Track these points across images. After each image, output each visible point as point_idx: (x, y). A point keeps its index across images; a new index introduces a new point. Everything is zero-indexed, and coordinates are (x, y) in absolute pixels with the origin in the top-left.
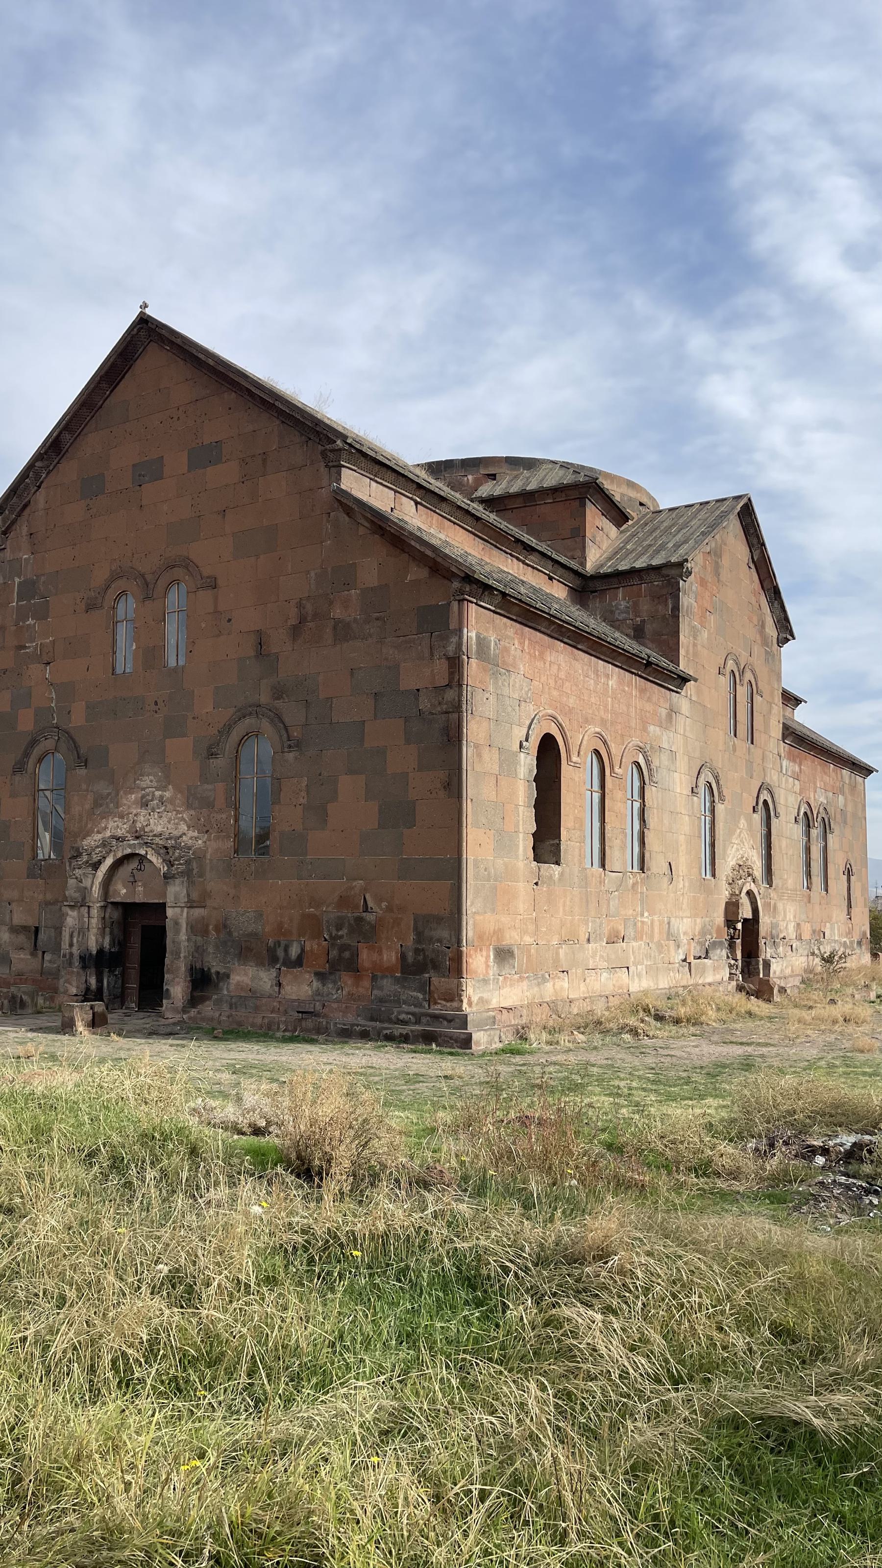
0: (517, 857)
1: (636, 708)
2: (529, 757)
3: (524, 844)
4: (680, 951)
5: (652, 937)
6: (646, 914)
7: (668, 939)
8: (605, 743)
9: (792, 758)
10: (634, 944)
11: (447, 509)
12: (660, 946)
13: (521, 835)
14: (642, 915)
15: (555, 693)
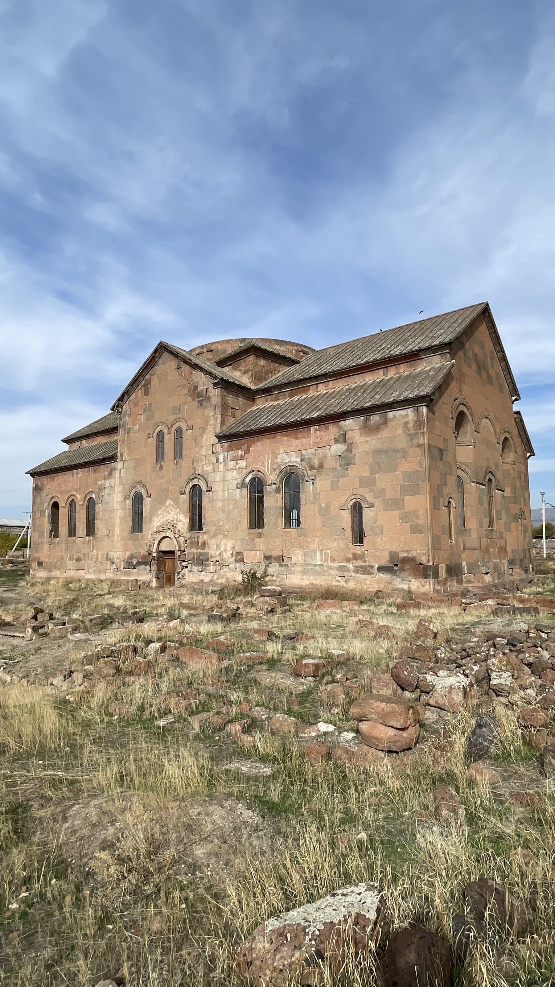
3: (47, 534)
6: (94, 551)
7: (107, 560)
12: (101, 563)
14: (92, 551)
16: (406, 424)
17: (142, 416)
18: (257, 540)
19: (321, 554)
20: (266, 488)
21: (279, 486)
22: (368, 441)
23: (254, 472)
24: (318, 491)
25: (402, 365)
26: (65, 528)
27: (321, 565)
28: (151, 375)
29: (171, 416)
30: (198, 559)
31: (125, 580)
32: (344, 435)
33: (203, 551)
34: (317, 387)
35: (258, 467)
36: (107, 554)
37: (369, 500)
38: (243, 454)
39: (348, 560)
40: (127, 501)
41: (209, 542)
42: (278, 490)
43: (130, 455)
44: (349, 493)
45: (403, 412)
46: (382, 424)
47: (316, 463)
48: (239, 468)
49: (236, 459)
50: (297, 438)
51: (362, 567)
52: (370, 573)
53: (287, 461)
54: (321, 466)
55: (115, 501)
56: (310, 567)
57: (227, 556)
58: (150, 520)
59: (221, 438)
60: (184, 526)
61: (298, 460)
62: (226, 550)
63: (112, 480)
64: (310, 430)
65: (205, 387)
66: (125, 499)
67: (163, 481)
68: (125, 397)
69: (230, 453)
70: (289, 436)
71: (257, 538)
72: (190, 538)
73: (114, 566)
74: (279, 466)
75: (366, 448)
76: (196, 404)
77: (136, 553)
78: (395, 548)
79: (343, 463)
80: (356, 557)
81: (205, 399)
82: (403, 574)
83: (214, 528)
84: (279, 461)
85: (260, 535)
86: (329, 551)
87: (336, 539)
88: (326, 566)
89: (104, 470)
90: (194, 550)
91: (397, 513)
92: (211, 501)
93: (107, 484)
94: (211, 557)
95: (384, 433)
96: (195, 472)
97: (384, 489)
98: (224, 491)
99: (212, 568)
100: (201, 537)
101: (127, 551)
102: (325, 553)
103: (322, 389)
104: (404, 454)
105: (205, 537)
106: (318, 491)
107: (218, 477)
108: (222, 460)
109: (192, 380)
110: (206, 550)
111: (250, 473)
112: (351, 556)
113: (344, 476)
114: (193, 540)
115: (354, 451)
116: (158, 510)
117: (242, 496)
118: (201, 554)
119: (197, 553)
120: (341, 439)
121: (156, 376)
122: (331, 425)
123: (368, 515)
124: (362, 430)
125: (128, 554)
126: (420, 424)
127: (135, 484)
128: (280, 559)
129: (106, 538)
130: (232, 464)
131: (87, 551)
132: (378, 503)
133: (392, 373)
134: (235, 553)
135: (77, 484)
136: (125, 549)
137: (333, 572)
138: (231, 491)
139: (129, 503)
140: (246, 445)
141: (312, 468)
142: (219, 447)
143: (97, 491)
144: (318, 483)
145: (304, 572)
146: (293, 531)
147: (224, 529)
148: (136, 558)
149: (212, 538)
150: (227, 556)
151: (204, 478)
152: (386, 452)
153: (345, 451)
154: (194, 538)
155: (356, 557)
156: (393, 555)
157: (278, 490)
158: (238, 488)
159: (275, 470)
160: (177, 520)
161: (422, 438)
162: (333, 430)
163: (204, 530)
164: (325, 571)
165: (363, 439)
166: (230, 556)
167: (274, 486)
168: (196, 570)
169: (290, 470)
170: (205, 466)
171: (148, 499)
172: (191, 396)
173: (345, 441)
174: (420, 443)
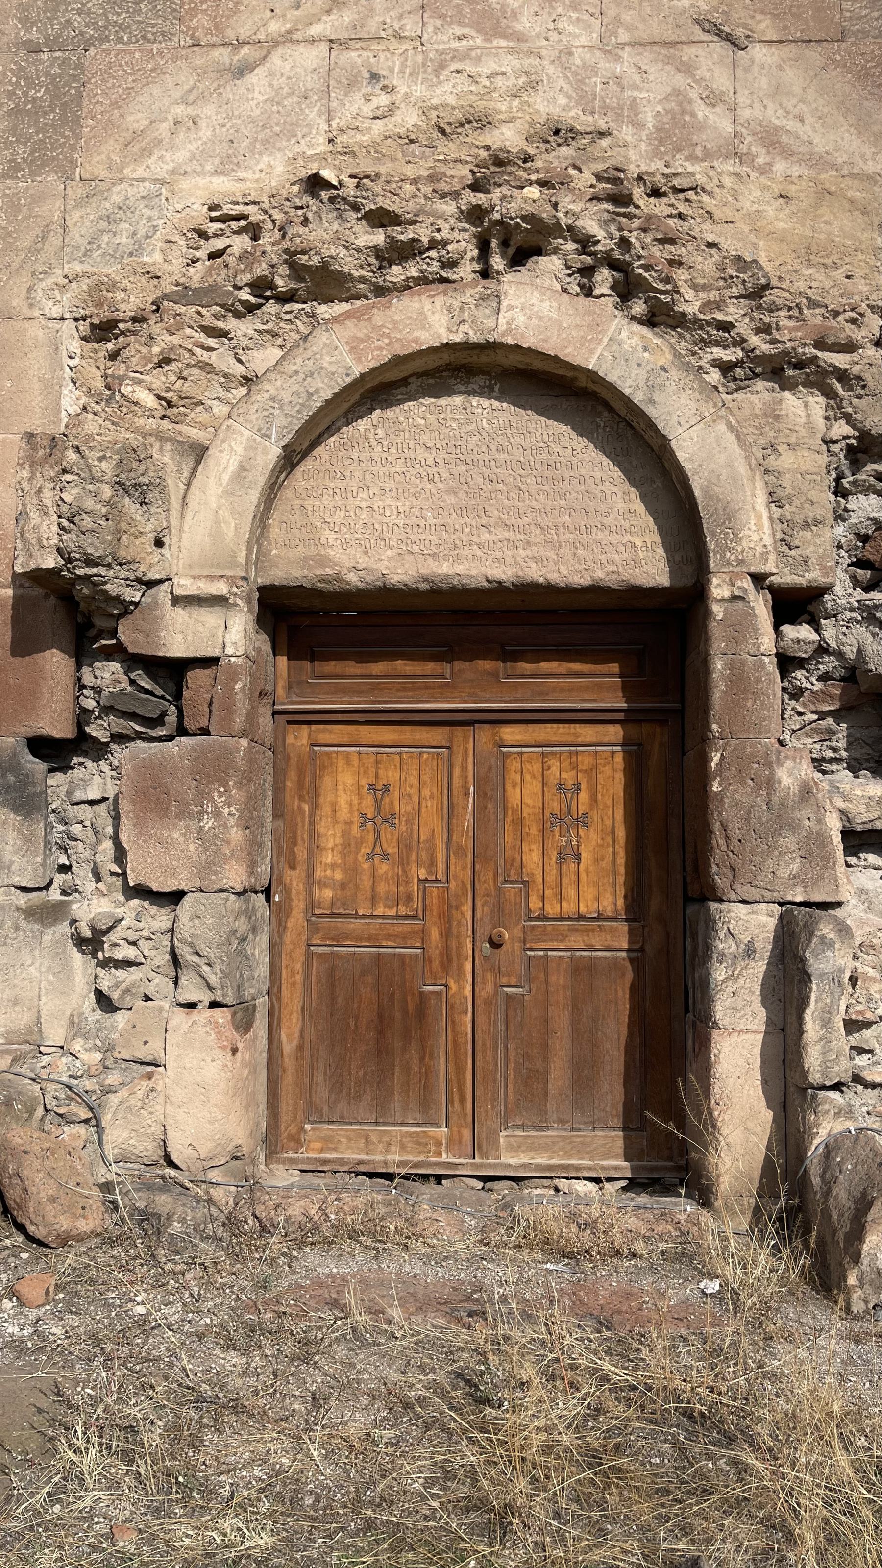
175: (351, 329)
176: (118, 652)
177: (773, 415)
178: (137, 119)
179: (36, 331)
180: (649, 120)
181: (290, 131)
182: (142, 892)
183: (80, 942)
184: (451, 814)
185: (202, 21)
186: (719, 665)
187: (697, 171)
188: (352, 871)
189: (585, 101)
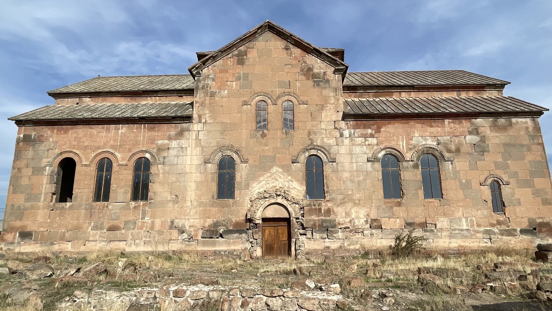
0: (39, 201)
1: (144, 136)
2: (52, 168)
4: (184, 234)
5: (152, 228)
8: (112, 154)
9: (355, 127)
10: (132, 231)
11: (104, 94)
12: (160, 233)
13: (43, 195)
15: (75, 143)
16: (527, 128)
17: (234, 83)
18: (395, 208)
19: (467, 221)
20: (402, 164)
21: (417, 163)
22: (497, 137)
23: (388, 150)
24: (458, 169)
25: (470, 92)
26: (86, 190)
27: (467, 230)
28: (248, 48)
29: (277, 89)
30: (321, 226)
31: (209, 251)
32: (477, 130)
33: (328, 218)
34: (400, 94)
35: (393, 144)
36: (172, 222)
37: (505, 179)
38: (373, 132)
39: (493, 225)
40: (209, 165)
41: (335, 209)
42: (416, 166)
43: (213, 117)
44: (486, 174)
45: (523, 120)
46: (508, 126)
47: (453, 148)
48: (369, 145)
49: (365, 136)
50: (431, 126)
51: (506, 230)
52: (514, 235)
53: (423, 143)
54: (458, 151)
55: (189, 163)
56: (457, 232)
57: (360, 222)
58: (247, 186)
59: (345, 117)
60: (299, 194)
61: (435, 143)
62: (357, 218)
63: (183, 141)
64: (444, 121)
65: (322, 71)
66: (206, 162)
67: (266, 148)
68: (210, 61)
69: (357, 130)
70: (423, 124)
71: (395, 206)
72: (308, 205)
73: (185, 236)
74: (415, 147)
75: (497, 141)
76: (310, 83)
77: (224, 221)
78: (532, 215)
79: (478, 150)
80: (499, 223)
81: (322, 81)
82: (541, 235)
83: (340, 197)
84: (414, 142)
85: (399, 204)
86: (474, 218)
87: (480, 209)
88: (473, 231)
89: (171, 129)
90: (315, 218)
91: (529, 190)
92: (336, 171)
93: (174, 144)
94: (339, 224)
95: (511, 132)
96: (312, 143)
97: (516, 172)
98: (352, 163)
99: (340, 234)
100: (323, 204)
101: (209, 218)
102: (471, 220)
103: (405, 96)
104: (529, 149)
105: (330, 205)
106: (458, 169)
107: (343, 150)
108: (348, 136)
109: (305, 62)
110: (332, 217)
111: (384, 149)
112: (495, 222)
113: (481, 160)
114: (313, 207)
115: (487, 142)
116: (259, 176)
117: (375, 170)
118: (323, 221)
119: (318, 220)
120: (475, 132)
121: (255, 50)
122: (464, 121)
123: (506, 191)
124: (492, 128)
125: (209, 222)
126: (537, 130)
127: (221, 149)
128: (423, 225)
129: (170, 205)
130: (360, 140)
131: (131, 218)
132: (512, 181)
133: (464, 95)
134: (369, 220)
135: (115, 141)
136: (205, 215)
137: (480, 235)
138: (360, 164)
139: (212, 168)
140: (376, 126)
141: (449, 151)
142: (343, 124)
143: (155, 150)
144: (457, 164)
145: (451, 237)
146: (435, 202)
147: (354, 198)
148: (225, 225)
149: (338, 206)
150: (360, 222)
151: (325, 149)
152: (514, 145)
153: (480, 141)
154: (315, 205)
155: (499, 223)
156: (531, 221)
157: (416, 166)
158: (368, 161)
159: (411, 149)
160: (289, 187)
161: (540, 139)
162: (466, 124)
163: (328, 198)
164: (472, 235)
165: (494, 134)
166: (364, 223)
167: (411, 163)
168: (318, 237)
169: (427, 151)
170: (325, 140)
171: (244, 165)
172: (305, 75)
173: (478, 134)
174: (540, 142)
175: (268, 202)
176: (253, 223)
177: (295, 206)
178: (253, 186)
179: (246, 201)
180: (287, 186)
181: (263, 187)
182: (255, 239)
183: (250, 242)
184: (275, 233)
185: (257, 179)
186: (291, 223)
187: (290, 190)
188: (268, 237)
189: (283, 185)
